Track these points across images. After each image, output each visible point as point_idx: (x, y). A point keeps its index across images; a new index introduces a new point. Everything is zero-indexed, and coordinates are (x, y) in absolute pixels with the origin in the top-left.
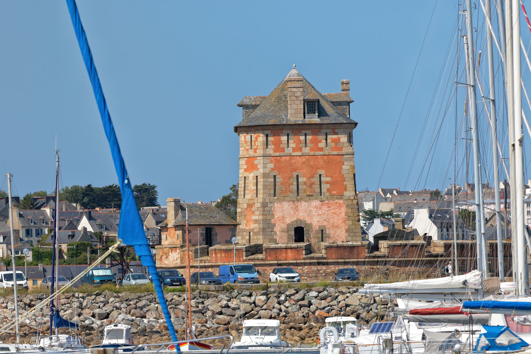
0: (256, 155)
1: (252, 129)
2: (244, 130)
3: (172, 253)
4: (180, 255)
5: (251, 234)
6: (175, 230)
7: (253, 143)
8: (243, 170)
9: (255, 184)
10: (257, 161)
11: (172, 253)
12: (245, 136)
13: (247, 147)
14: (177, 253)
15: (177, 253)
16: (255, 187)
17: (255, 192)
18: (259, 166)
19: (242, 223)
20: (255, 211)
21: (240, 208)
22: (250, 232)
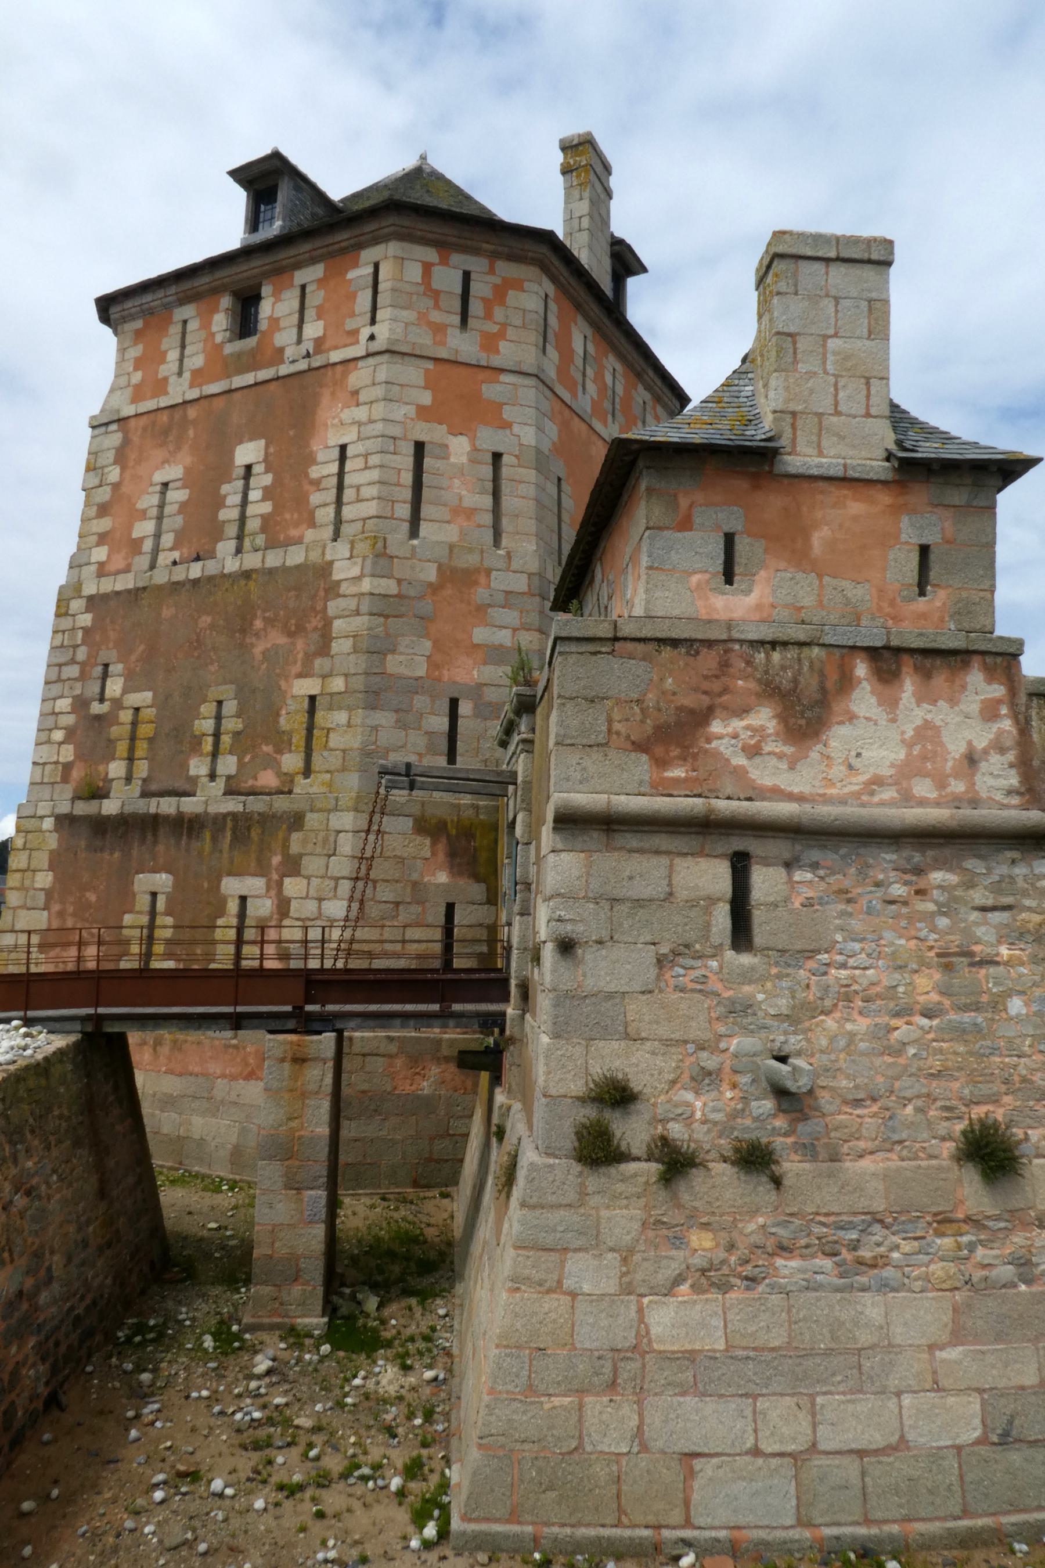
0: (496, 361)
1: (485, 246)
2: (430, 236)
3: (891, 704)
4: (1007, 724)
5: (465, 708)
6: (896, 510)
7: (476, 307)
8: (411, 411)
9: (489, 486)
10: (498, 388)
11: (891, 704)
12: (427, 268)
13: (436, 316)
14: (972, 703)
15: (972, 703)
16: (488, 501)
17: (488, 519)
18: (507, 413)
19: (401, 649)
20: (489, 606)
21: (390, 576)
22: (454, 703)
